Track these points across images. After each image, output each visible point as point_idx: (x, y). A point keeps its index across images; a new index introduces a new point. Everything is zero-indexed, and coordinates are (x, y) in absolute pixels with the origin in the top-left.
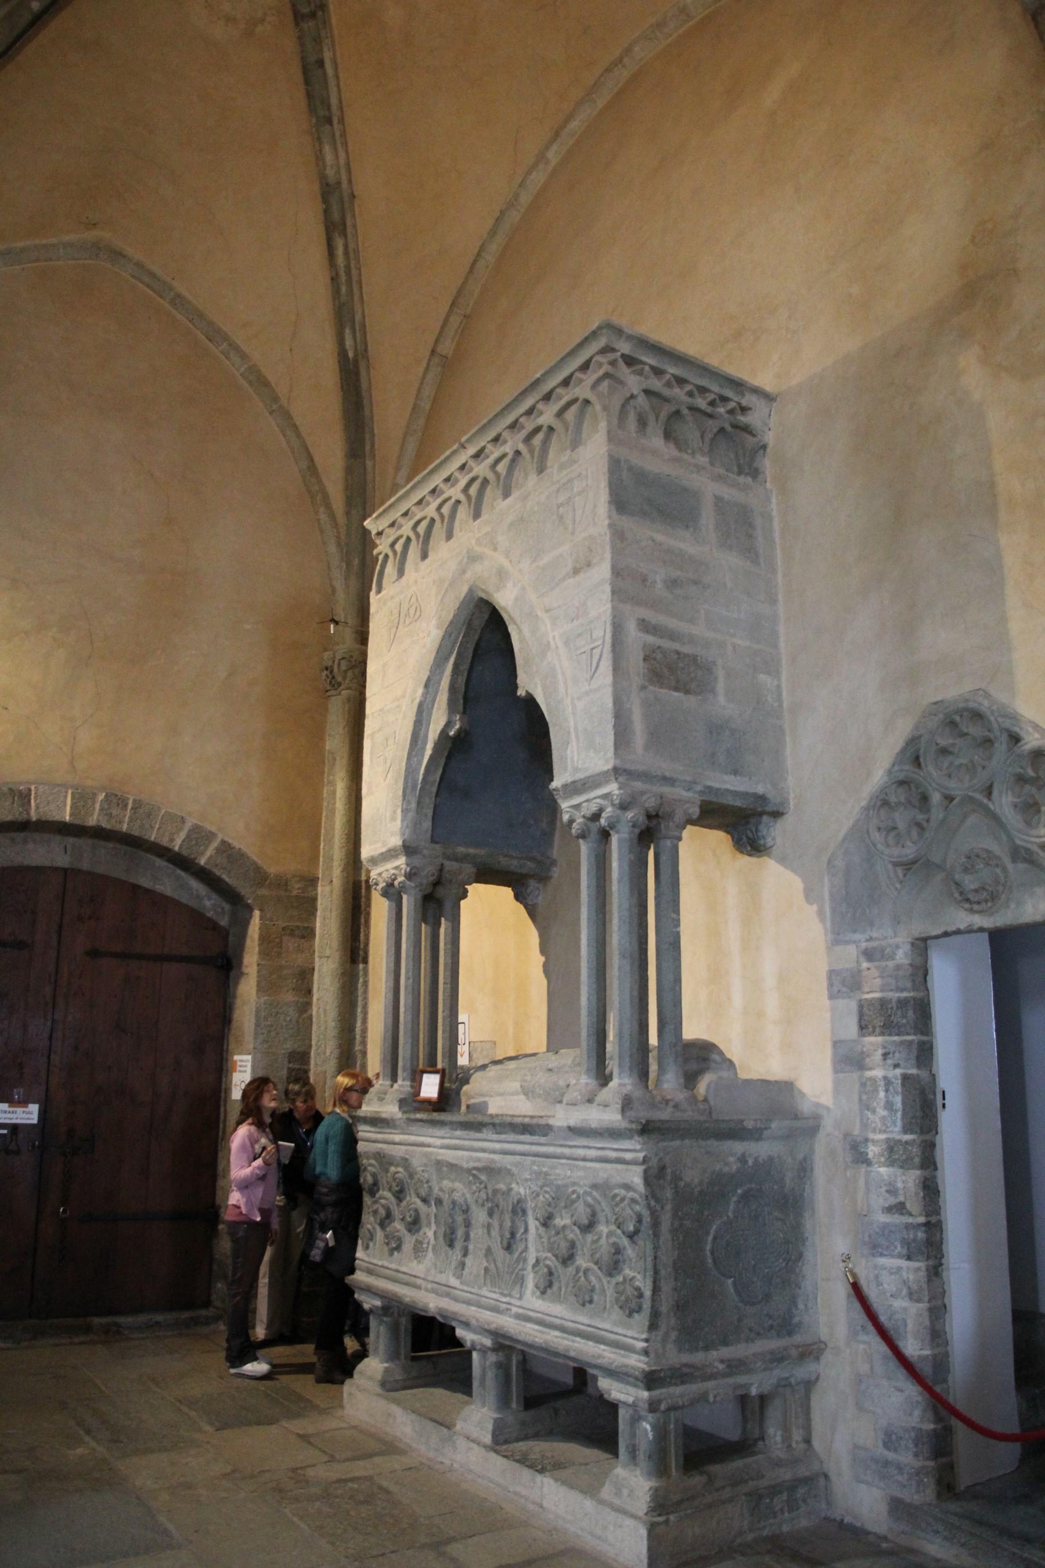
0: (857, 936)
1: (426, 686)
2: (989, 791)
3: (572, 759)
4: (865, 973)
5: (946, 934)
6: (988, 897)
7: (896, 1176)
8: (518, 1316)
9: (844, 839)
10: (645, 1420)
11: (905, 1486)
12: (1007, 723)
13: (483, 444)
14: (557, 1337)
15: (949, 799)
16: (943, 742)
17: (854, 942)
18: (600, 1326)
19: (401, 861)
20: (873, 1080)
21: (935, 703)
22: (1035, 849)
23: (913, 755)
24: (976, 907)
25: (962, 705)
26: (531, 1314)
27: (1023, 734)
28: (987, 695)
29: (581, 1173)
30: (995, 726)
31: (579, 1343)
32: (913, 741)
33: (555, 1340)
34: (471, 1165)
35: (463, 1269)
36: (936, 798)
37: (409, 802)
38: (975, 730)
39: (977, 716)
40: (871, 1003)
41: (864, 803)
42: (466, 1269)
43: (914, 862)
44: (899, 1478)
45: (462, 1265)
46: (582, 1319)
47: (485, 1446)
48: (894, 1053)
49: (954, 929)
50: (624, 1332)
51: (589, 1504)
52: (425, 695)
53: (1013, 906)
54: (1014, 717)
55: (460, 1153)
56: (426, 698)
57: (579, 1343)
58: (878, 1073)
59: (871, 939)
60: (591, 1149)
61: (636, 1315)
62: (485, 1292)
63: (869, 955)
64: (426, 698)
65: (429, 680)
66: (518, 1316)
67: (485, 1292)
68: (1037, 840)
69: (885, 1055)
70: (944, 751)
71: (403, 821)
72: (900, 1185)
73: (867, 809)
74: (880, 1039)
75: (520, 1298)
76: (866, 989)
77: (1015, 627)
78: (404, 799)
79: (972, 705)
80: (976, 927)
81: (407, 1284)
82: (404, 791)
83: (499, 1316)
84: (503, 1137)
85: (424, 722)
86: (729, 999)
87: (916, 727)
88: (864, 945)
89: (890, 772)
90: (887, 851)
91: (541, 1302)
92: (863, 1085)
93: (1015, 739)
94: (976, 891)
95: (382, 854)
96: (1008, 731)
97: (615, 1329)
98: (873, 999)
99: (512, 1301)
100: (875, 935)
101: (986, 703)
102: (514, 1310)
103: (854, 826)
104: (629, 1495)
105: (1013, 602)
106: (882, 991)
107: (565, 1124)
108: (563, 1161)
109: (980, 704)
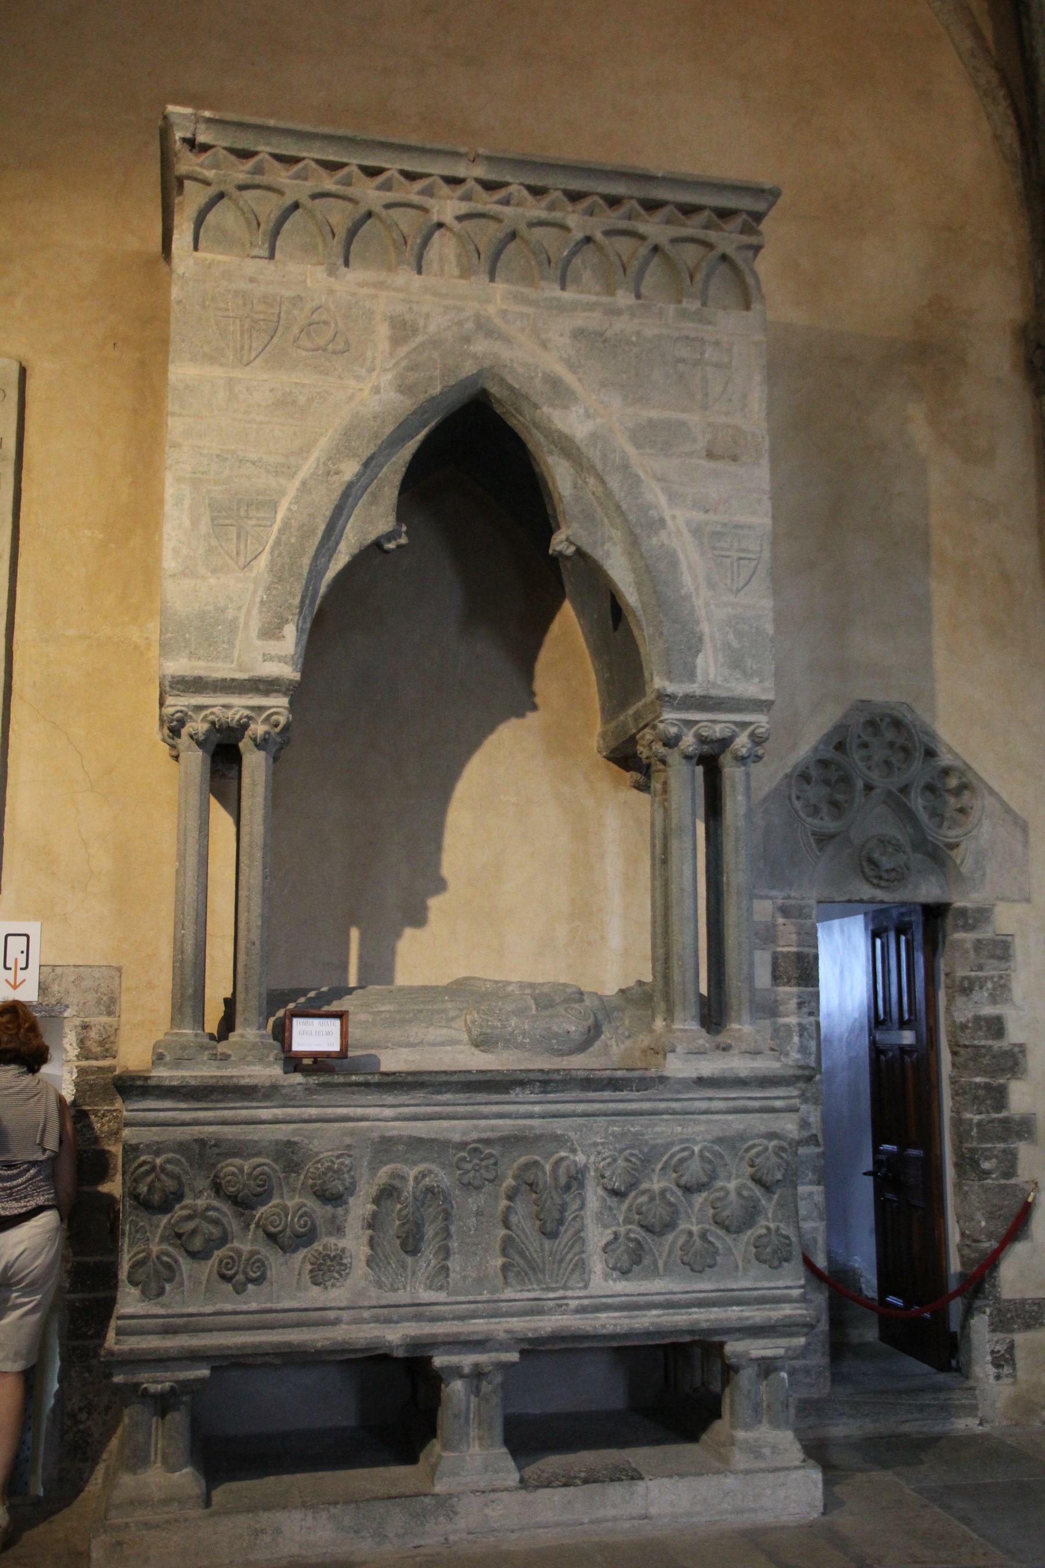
0: (773, 893)
1: (366, 465)
2: (905, 789)
3: (706, 672)
4: (781, 928)
5: (849, 901)
6: (898, 877)
7: (808, 1112)
8: (582, 1310)
9: (765, 799)
10: (782, 1370)
11: (813, 1386)
12: (926, 739)
13: (508, 178)
14: (659, 1316)
15: (869, 788)
16: (865, 738)
17: (771, 898)
18: (735, 1287)
19: (279, 702)
20: (787, 1026)
21: (863, 701)
22: (941, 845)
23: (838, 742)
24: (883, 883)
25: (888, 711)
26: (609, 1300)
27: (939, 752)
28: (912, 711)
29: (702, 1128)
30: (916, 738)
31: (696, 1313)
32: (841, 728)
33: (658, 1320)
34: (475, 1136)
35: (448, 1276)
36: (860, 784)
37: (304, 622)
38: (889, 735)
39: (897, 724)
40: (786, 955)
41: (788, 770)
42: (452, 1275)
43: (832, 836)
44: (808, 1380)
45: (445, 1270)
46: (705, 1285)
47: (517, 1489)
48: (809, 1002)
49: (858, 898)
50: (773, 1285)
51: (730, 1482)
52: (359, 476)
53: (910, 887)
54: (933, 736)
55: (445, 1124)
56: (358, 480)
57: (696, 1313)
58: (793, 1020)
59: (789, 897)
60: (719, 1099)
61: (785, 1264)
62: (509, 1294)
63: (785, 911)
64: (358, 480)
65: (371, 458)
66: (582, 1310)
67: (509, 1294)
68: (947, 840)
69: (800, 1005)
70: (865, 745)
71: (297, 645)
72: (812, 1119)
73: (787, 776)
74: (795, 990)
75: (586, 1287)
76: (781, 943)
77: (939, 662)
78: (300, 613)
79: (895, 713)
80: (878, 899)
81: (298, 1325)
82: (302, 602)
83: (546, 1317)
84: (551, 1096)
85: (345, 512)
86: (602, 938)
87: (845, 716)
88: (780, 902)
89: (816, 749)
90: (809, 820)
91: (624, 1283)
92: (776, 1031)
93: (930, 754)
94: (887, 871)
95: (224, 680)
96: (926, 745)
97: (759, 1285)
98: (788, 952)
99: (569, 1293)
100: (793, 894)
101: (909, 716)
102: (573, 1304)
103: (776, 789)
104: (773, 1453)
105: (938, 641)
106: (798, 946)
107: (695, 1075)
108: (665, 1117)
109: (904, 716)
